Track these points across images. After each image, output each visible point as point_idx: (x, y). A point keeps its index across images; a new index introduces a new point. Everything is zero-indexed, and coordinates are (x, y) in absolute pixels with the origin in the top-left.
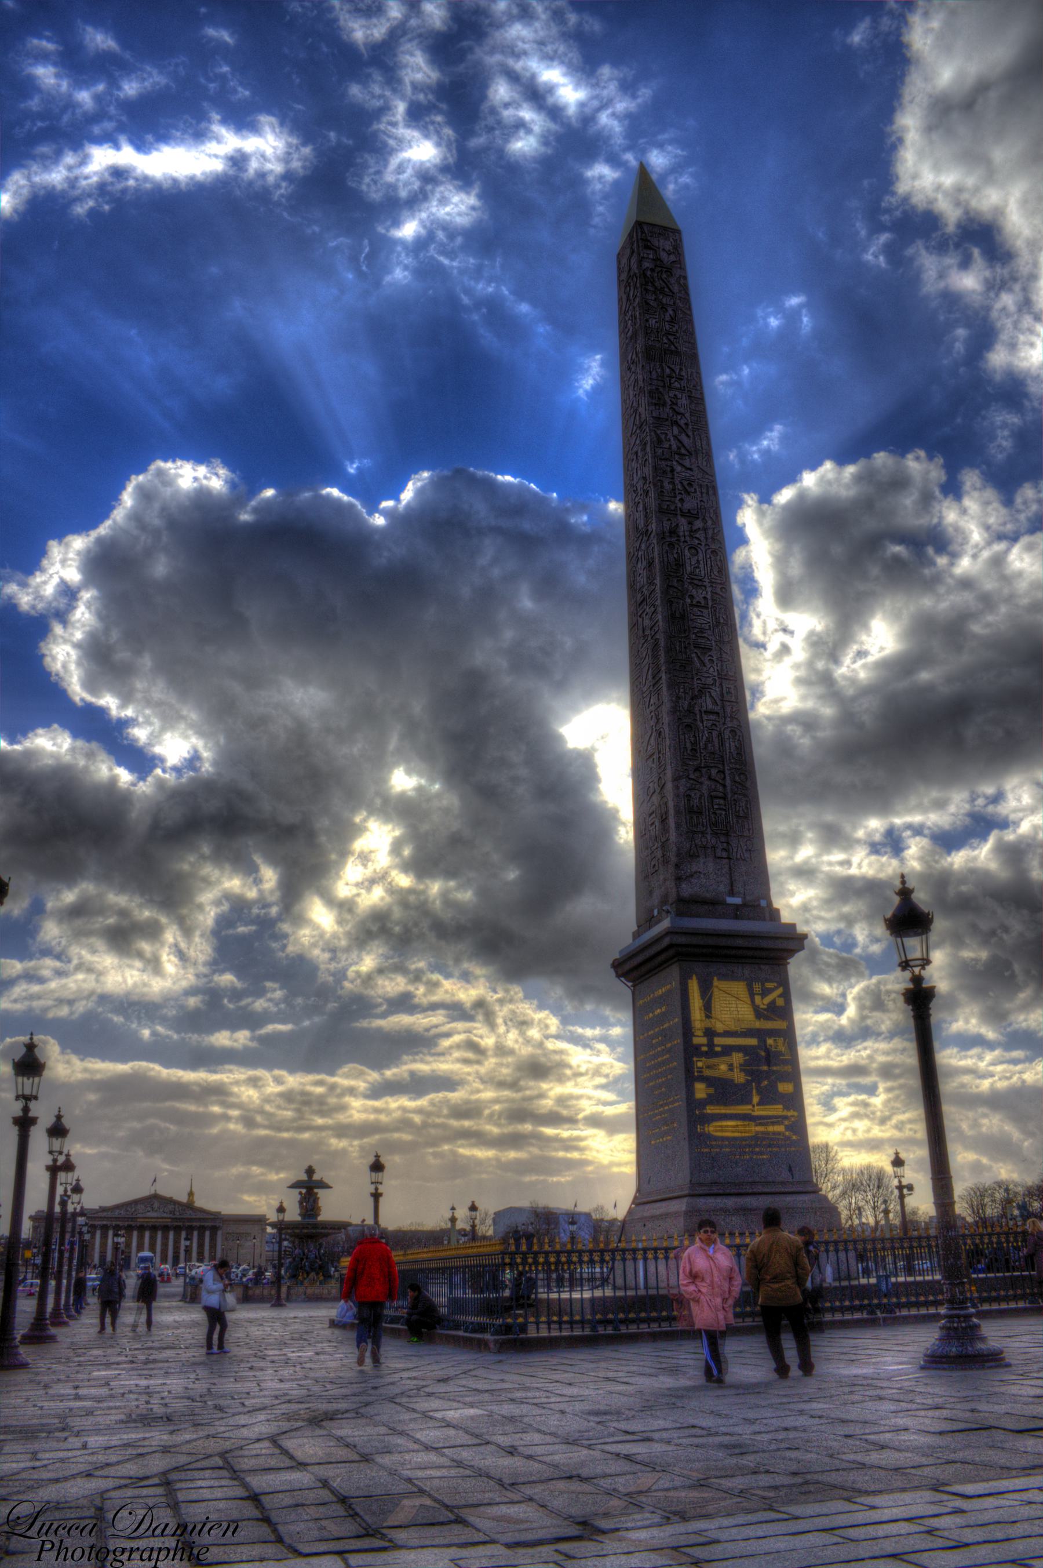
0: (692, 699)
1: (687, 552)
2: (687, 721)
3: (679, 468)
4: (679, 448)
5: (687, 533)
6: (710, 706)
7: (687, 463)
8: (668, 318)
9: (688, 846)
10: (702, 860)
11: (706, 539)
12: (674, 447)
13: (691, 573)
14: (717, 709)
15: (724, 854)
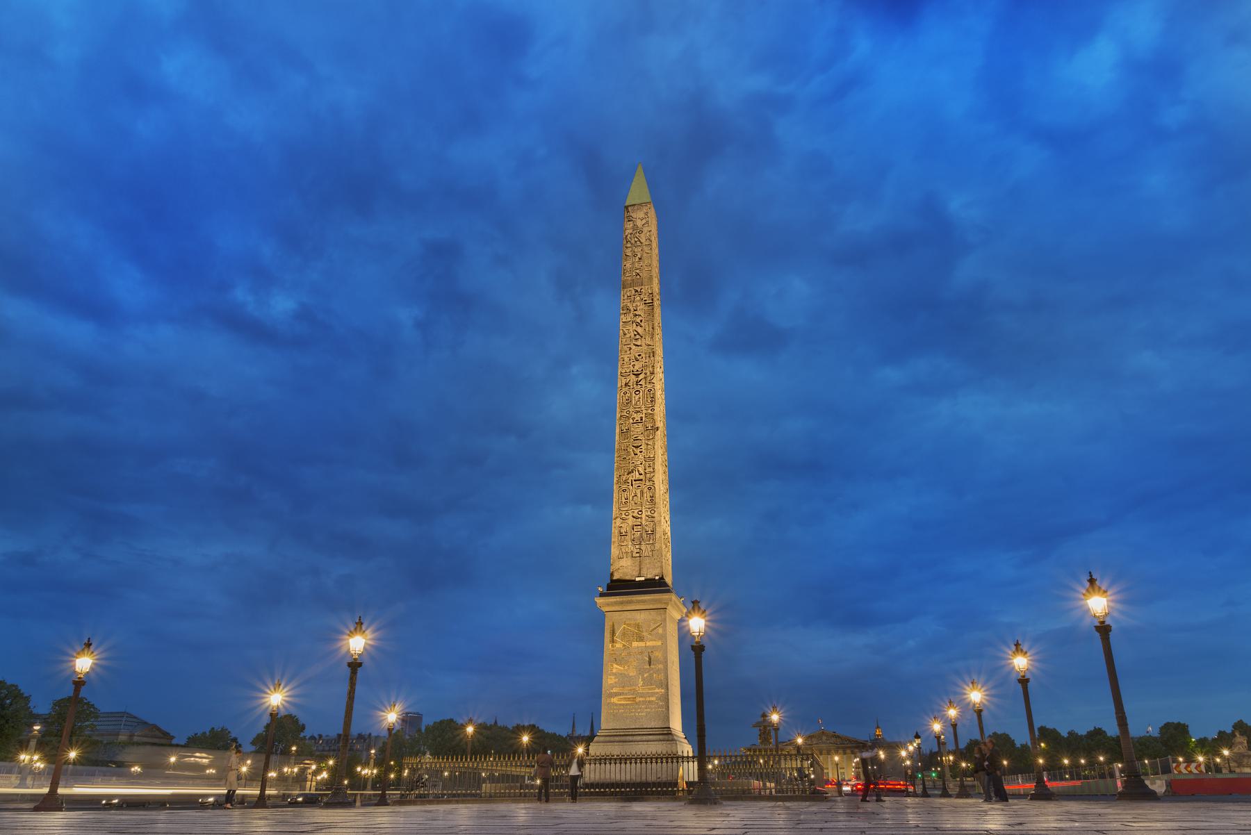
0: (628, 474)
1: (634, 395)
2: (624, 487)
3: (634, 347)
4: (635, 335)
5: (635, 383)
6: (638, 476)
7: (639, 343)
8: (637, 259)
9: (618, 553)
10: (625, 559)
11: (646, 383)
12: (633, 336)
13: (636, 404)
14: (641, 477)
15: (638, 555)
